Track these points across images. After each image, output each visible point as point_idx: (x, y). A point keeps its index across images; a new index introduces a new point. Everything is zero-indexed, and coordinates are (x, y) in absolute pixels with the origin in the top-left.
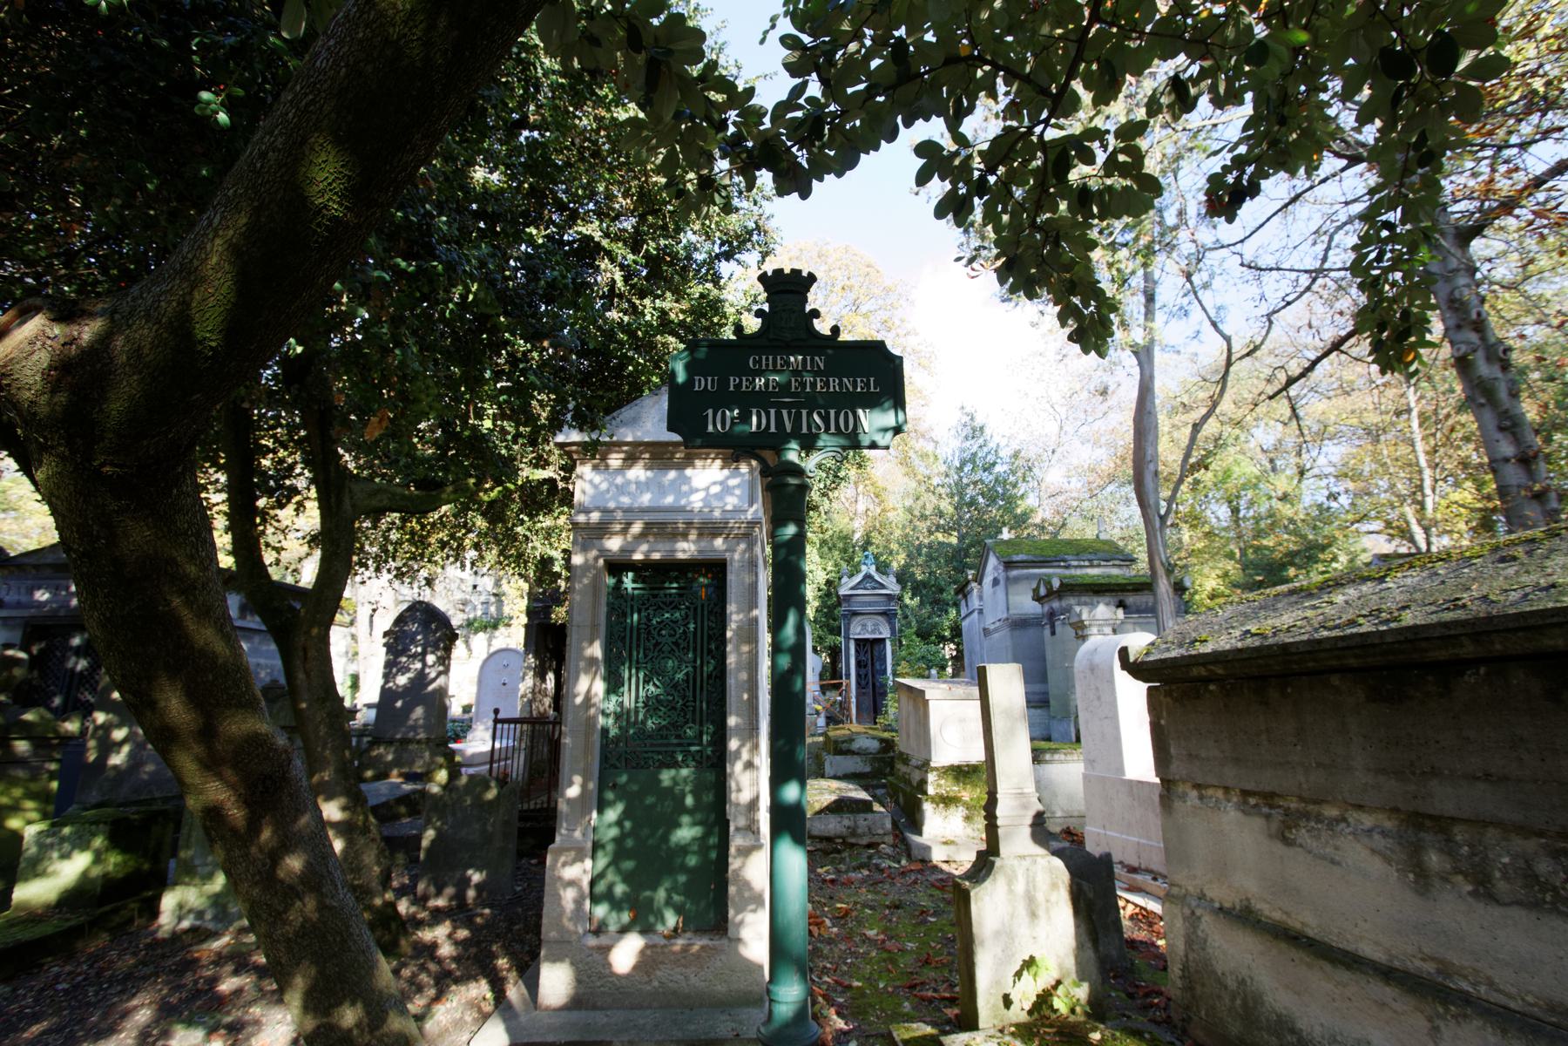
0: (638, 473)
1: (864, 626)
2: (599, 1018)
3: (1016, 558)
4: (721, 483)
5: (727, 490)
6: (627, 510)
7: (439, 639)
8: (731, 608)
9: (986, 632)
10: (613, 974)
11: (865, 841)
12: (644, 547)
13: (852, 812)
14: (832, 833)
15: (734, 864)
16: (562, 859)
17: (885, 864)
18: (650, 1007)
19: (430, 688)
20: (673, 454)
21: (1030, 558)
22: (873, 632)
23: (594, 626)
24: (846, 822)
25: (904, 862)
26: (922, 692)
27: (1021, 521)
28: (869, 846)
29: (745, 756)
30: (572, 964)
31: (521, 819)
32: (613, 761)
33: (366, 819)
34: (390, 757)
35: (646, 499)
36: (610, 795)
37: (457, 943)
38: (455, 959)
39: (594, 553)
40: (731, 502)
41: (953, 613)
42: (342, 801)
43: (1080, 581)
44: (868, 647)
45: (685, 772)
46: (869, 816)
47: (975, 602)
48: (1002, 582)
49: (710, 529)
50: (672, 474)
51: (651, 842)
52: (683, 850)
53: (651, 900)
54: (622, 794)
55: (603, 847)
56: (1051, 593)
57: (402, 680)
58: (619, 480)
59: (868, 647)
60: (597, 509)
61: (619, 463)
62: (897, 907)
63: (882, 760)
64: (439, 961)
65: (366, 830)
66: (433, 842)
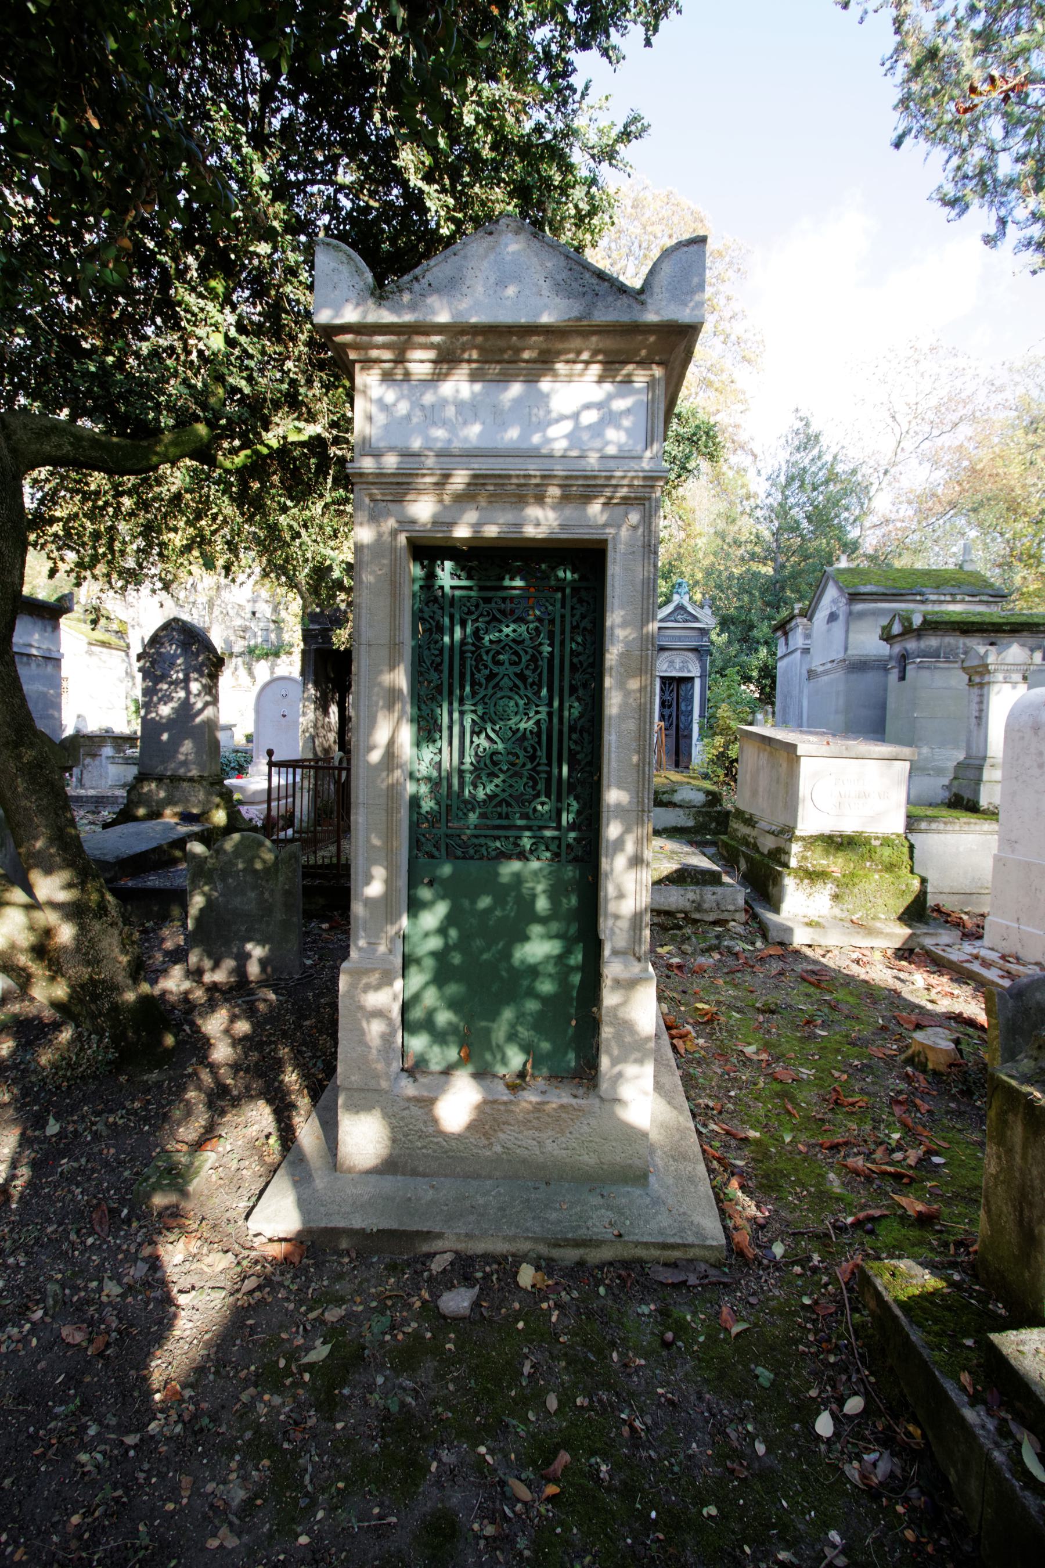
0: (459, 386)
1: (672, 662)
2: (423, 1191)
3: (863, 589)
4: (599, 406)
5: (610, 418)
6: (443, 454)
7: (202, 664)
8: (615, 617)
9: (811, 674)
10: (441, 1133)
11: (711, 918)
12: (471, 516)
13: (697, 884)
14: (673, 908)
15: (610, 998)
16: (365, 980)
17: (739, 946)
18: (490, 1177)
19: (198, 720)
20: (518, 351)
21: (881, 590)
22: (681, 669)
23: (394, 646)
24: (691, 896)
25: (759, 944)
26: (793, 747)
27: (851, 548)
28: (716, 923)
29: (630, 847)
30: (386, 1115)
31: (305, 875)
32: (429, 848)
33: (103, 896)
34: (162, 794)
35: (473, 432)
36: (425, 893)
37: (236, 1042)
38: (236, 1067)
39: (391, 523)
40: (615, 438)
41: (763, 652)
42: (62, 877)
43: (946, 618)
44: (674, 686)
45: (535, 865)
46: (719, 890)
47: (798, 639)
48: (842, 618)
49: (580, 488)
50: (516, 389)
51: (485, 956)
52: (533, 971)
53: (488, 1031)
54: (446, 889)
55: (418, 961)
56: (908, 631)
57: (165, 710)
58: (428, 398)
59: (674, 686)
60: (391, 449)
61: (427, 368)
62: (773, 1012)
63: (707, 814)
64: (213, 1067)
65: (102, 909)
66: (201, 910)
